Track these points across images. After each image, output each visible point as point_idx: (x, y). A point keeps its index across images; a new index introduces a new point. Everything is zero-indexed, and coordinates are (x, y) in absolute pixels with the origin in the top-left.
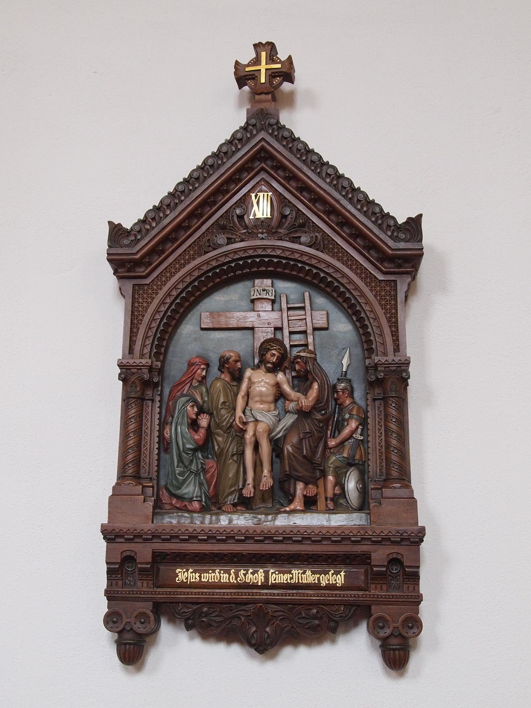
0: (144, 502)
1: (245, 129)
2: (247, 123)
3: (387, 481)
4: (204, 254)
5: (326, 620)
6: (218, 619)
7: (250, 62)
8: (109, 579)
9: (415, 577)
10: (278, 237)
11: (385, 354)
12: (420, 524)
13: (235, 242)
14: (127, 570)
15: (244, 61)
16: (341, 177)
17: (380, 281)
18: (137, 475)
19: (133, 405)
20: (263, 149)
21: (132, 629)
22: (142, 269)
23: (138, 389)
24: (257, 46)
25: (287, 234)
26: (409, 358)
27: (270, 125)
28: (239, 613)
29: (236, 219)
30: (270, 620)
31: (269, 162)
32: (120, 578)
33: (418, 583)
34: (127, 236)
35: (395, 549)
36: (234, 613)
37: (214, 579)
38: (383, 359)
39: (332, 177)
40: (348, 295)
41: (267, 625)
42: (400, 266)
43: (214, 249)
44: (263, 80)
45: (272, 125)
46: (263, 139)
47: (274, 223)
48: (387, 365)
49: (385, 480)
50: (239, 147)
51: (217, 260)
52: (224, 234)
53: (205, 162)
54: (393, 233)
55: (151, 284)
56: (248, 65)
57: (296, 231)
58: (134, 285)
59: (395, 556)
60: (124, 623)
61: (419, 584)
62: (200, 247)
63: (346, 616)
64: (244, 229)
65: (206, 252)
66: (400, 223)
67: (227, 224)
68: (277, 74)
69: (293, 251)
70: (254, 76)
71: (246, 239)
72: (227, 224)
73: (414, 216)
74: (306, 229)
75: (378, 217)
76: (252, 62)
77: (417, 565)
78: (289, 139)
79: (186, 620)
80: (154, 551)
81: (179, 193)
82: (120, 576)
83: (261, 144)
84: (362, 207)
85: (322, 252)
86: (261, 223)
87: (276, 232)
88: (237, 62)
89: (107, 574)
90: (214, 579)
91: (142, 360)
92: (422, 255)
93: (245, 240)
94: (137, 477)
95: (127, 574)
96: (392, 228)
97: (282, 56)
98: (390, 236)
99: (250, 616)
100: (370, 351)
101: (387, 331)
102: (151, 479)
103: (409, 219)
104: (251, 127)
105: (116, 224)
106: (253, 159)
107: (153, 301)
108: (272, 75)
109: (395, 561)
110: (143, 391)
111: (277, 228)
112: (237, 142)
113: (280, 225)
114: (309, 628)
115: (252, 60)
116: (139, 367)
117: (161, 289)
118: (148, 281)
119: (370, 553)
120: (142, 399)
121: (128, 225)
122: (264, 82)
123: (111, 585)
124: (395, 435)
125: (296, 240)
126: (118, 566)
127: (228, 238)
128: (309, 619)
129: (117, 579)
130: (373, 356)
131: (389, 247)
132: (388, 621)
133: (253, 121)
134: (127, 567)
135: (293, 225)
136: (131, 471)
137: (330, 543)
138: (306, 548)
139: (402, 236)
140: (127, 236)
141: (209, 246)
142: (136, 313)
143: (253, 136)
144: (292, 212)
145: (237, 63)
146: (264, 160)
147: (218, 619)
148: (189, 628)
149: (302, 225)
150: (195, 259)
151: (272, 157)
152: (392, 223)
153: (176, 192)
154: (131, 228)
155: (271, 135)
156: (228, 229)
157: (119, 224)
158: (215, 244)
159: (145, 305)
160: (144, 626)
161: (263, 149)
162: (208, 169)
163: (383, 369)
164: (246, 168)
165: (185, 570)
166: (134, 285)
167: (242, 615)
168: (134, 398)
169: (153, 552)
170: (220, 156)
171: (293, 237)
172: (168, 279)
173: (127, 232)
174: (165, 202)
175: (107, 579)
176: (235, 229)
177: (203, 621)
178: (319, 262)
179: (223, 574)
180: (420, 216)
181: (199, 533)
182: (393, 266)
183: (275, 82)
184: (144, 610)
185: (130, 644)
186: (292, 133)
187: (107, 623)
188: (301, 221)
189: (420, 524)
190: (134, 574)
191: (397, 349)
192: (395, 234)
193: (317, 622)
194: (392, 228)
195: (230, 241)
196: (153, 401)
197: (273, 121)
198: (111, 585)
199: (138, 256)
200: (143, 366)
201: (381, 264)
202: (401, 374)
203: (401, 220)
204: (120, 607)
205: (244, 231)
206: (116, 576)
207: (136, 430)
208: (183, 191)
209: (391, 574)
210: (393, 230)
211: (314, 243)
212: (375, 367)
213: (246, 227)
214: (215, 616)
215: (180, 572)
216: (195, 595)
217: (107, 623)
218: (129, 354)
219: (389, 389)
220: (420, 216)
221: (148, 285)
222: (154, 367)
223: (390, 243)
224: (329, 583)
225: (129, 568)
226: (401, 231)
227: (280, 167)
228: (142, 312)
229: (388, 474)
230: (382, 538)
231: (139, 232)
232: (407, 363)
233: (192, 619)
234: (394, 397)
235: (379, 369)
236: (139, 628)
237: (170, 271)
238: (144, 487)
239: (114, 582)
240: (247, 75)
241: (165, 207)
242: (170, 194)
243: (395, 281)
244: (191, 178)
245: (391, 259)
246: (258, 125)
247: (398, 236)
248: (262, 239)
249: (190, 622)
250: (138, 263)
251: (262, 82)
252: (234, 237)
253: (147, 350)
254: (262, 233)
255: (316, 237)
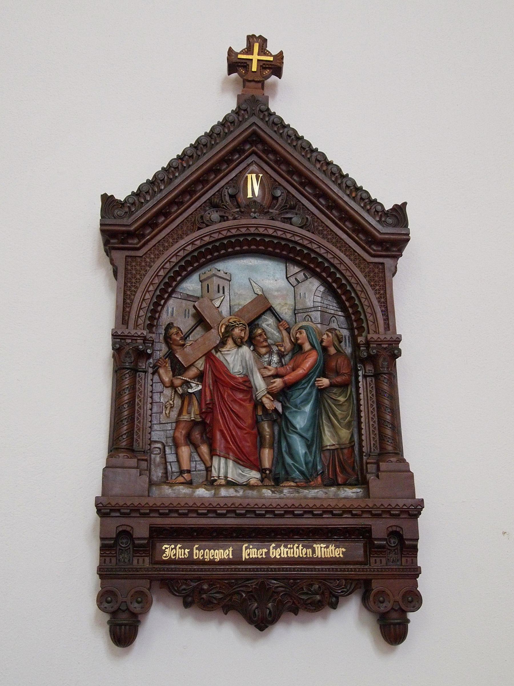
0: (140, 475)
1: (237, 112)
2: (239, 107)
3: (383, 454)
4: (198, 230)
5: (327, 594)
6: (219, 596)
7: (242, 51)
8: (102, 556)
9: (414, 549)
10: (270, 217)
11: (376, 332)
12: (418, 496)
13: (228, 219)
14: (121, 546)
15: (237, 49)
16: (329, 163)
17: (368, 263)
18: (130, 448)
19: (127, 376)
20: (254, 133)
21: (128, 609)
22: (136, 241)
23: (133, 359)
24: (249, 37)
25: (279, 214)
26: (401, 336)
27: (261, 111)
28: (239, 589)
29: (227, 198)
30: (272, 596)
31: (260, 146)
32: (114, 555)
33: (416, 556)
34: (121, 207)
35: (393, 522)
36: (235, 588)
37: (257, 555)
38: (375, 337)
39: (321, 162)
40: (338, 276)
41: (268, 601)
42: (387, 250)
43: (207, 226)
44: (254, 68)
45: (262, 112)
46: (254, 124)
47: (266, 202)
48: (379, 343)
49: (379, 455)
50: (232, 129)
51: (211, 236)
52: (217, 212)
53: (198, 142)
54: (380, 219)
55: (144, 256)
56: (240, 53)
57: (287, 213)
58: (126, 256)
59: (394, 529)
60: (119, 602)
61: (417, 557)
62: (194, 223)
63: (348, 591)
64: (237, 208)
65: (199, 229)
66: (386, 209)
67: (220, 202)
68: (267, 66)
69: (285, 231)
70: (245, 64)
71: (239, 218)
72: (220, 202)
73: (400, 204)
74: (296, 211)
75: (366, 202)
76: (244, 51)
77: (415, 538)
78: (279, 125)
79: (185, 598)
80: (151, 526)
81: (173, 169)
82: (114, 552)
83: (252, 128)
84: (351, 192)
85: (313, 233)
86: (253, 202)
87: (268, 212)
88: (230, 48)
89: (101, 550)
90: (257, 555)
91: (135, 331)
92: (408, 240)
93: (238, 218)
94: (131, 450)
95: (121, 551)
96: (380, 214)
97: (273, 48)
98: (378, 221)
99: (251, 592)
100: (361, 329)
101: (378, 310)
102: (144, 452)
103: (396, 205)
104: (243, 112)
105: (109, 195)
106: (245, 141)
107: (146, 273)
108: (263, 65)
109: (396, 534)
110: (136, 362)
111: (269, 208)
112: (229, 124)
113: (271, 206)
114: (310, 603)
115: (244, 49)
116: (134, 338)
117: (154, 262)
118: (140, 253)
119: (370, 526)
120: (135, 371)
121: (121, 196)
122: (255, 70)
123: (105, 562)
124: (389, 410)
125: (289, 220)
126: (113, 542)
127: (220, 216)
128: (310, 594)
129: (110, 556)
130: (364, 334)
131: (378, 231)
132: (389, 596)
133: (244, 106)
134: (121, 543)
135: (284, 206)
136: (124, 444)
137: (330, 516)
138: (327, 521)
139: (390, 221)
140: (121, 207)
141: (203, 223)
142: (129, 284)
143: (245, 120)
144: (282, 194)
145: (230, 50)
146: (253, 143)
147: (219, 596)
148: (187, 605)
149: (293, 208)
150: (188, 235)
151: (263, 141)
152: (379, 208)
153: (169, 168)
154: (125, 199)
155: (262, 120)
156: (221, 208)
157: (112, 196)
158: (208, 221)
159: (138, 277)
160: (140, 605)
161: (254, 133)
162: (201, 148)
163: (375, 345)
164: (238, 150)
165: (173, 546)
166: (126, 256)
167: (242, 591)
168: (128, 369)
169: (150, 527)
170: (213, 137)
171: (285, 218)
172: (161, 253)
173: (121, 204)
174: (159, 176)
175: (100, 556)
176: (228, 208)
177: (203, 598)
178: (310, 243)
179: (252, 549)
180: (405, 204)
181: (199, 507)
182: (380, 249)
183: (264, 73)
184: (142, 589)
185: (125, 625)
186: (282, 120)
187: (101, 603)
188: (292, 203)
189: (417, 497)
190: (128, 551)
191: (387, 327)
192: (383, 219)
193: (318, 597)
194: (380, 214)
195: (223, 219)
196: (145, 372)
197: (263, 107)
198: (105, 562)
199: (132, 228)
200: (139, 336)
201: (370, 247)
202: (394, 351)
203: (388, 207)
204: (116, 584)
205: (238, 210)
206: (111, 553)
207: (130, 402)
208: (178, 168)
209: (389, 548)
210: (381, 215)
211: (305, 224)
212: (368, 343)
213: (238, 206)
214: (213, 593)
215: (166, 548)
216: (182, 571)
217: (101, 603)
218: (123, 324)
219: (380, 366)
220: (405, 204)
221: (142, 257)
222: (148, 337)
223: (379, 227)
224: (249, 557)
225: (123, 544)
226: (388, 216)
227: (270, 150)
228: (135, 283)
229: (382, 448)
230: (382, 511)
231: (134, 204)
232: (398, 340)
233: (192, 597)
234: (387, 373)
235: (371, 345)
236: (135, 608)
237: (164, 245)
238: (138, 460)
239: (108, 559)
240: (239, 62)
241: (159, 182)
242: (163, 168)
243: (383, 264)
244: (185, 155)
245: (380, 243)
246: (249, 109)
247: (386, 222)
248: (255, 218)
249: (190, 599)
250: (131, 235)
251: (253, 70)
252: (227, 215)
253: (140, 321)
254: (255, 212)
255: (307, 218)
